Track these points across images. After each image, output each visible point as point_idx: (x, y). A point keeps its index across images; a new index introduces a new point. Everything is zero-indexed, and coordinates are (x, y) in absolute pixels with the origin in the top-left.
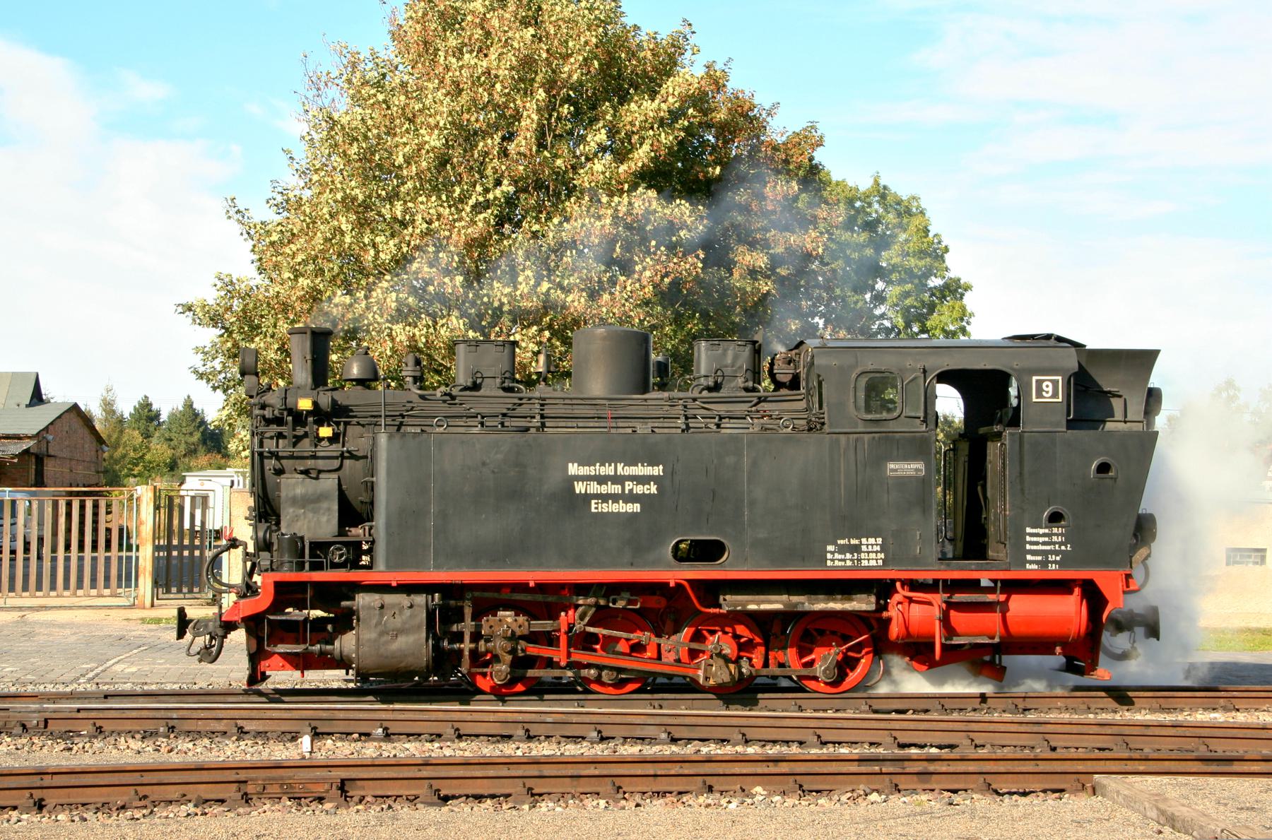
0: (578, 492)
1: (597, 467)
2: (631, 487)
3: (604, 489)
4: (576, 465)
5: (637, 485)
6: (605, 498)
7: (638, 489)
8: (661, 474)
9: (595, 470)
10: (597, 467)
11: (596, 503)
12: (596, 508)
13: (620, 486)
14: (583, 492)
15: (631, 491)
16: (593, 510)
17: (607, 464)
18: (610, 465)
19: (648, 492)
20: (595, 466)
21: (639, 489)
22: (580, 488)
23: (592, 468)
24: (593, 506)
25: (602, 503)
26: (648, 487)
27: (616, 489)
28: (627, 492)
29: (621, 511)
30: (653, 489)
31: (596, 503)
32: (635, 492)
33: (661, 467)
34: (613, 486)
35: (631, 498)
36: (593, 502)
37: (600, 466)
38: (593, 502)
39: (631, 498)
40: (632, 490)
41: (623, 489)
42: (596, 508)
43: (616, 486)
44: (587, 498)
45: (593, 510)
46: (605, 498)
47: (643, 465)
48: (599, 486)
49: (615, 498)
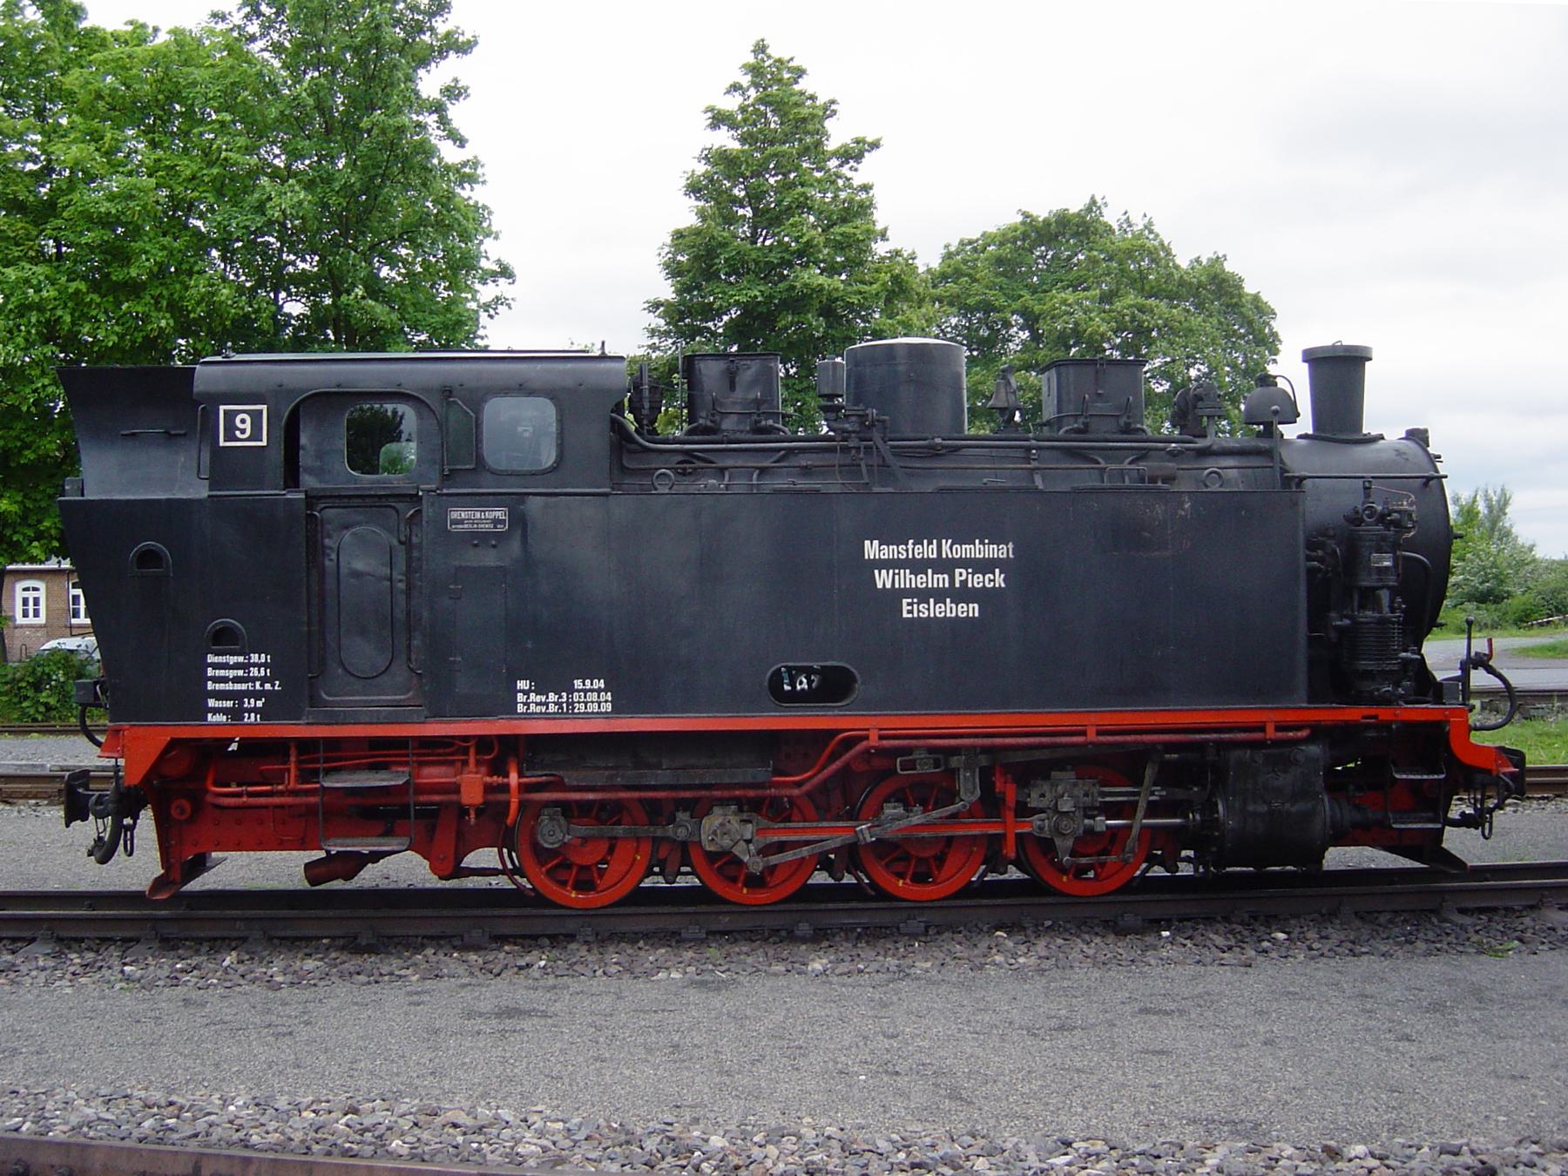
0: (880, 586)
1: (910, 546)
3: (920, 581)
4: (876, 542)
6: (923, 595)
8: (1011, 556)
9: (907, 550)
10: (910, 546)
11: (909, 604)
14: (888, 586)
16: (905, 615)
20: (907, 544)
21: (976, 581)
22: (883, 579)
24: (905, 608)
25: (918, 604)
31: (909, 604)
32: (970, 585)
33: (1011, 546)
34: (935, 576)
36: (905, 601)
37: (914, 544)
38: (905, 601)
44: (897, 595)
46: (923, 595)
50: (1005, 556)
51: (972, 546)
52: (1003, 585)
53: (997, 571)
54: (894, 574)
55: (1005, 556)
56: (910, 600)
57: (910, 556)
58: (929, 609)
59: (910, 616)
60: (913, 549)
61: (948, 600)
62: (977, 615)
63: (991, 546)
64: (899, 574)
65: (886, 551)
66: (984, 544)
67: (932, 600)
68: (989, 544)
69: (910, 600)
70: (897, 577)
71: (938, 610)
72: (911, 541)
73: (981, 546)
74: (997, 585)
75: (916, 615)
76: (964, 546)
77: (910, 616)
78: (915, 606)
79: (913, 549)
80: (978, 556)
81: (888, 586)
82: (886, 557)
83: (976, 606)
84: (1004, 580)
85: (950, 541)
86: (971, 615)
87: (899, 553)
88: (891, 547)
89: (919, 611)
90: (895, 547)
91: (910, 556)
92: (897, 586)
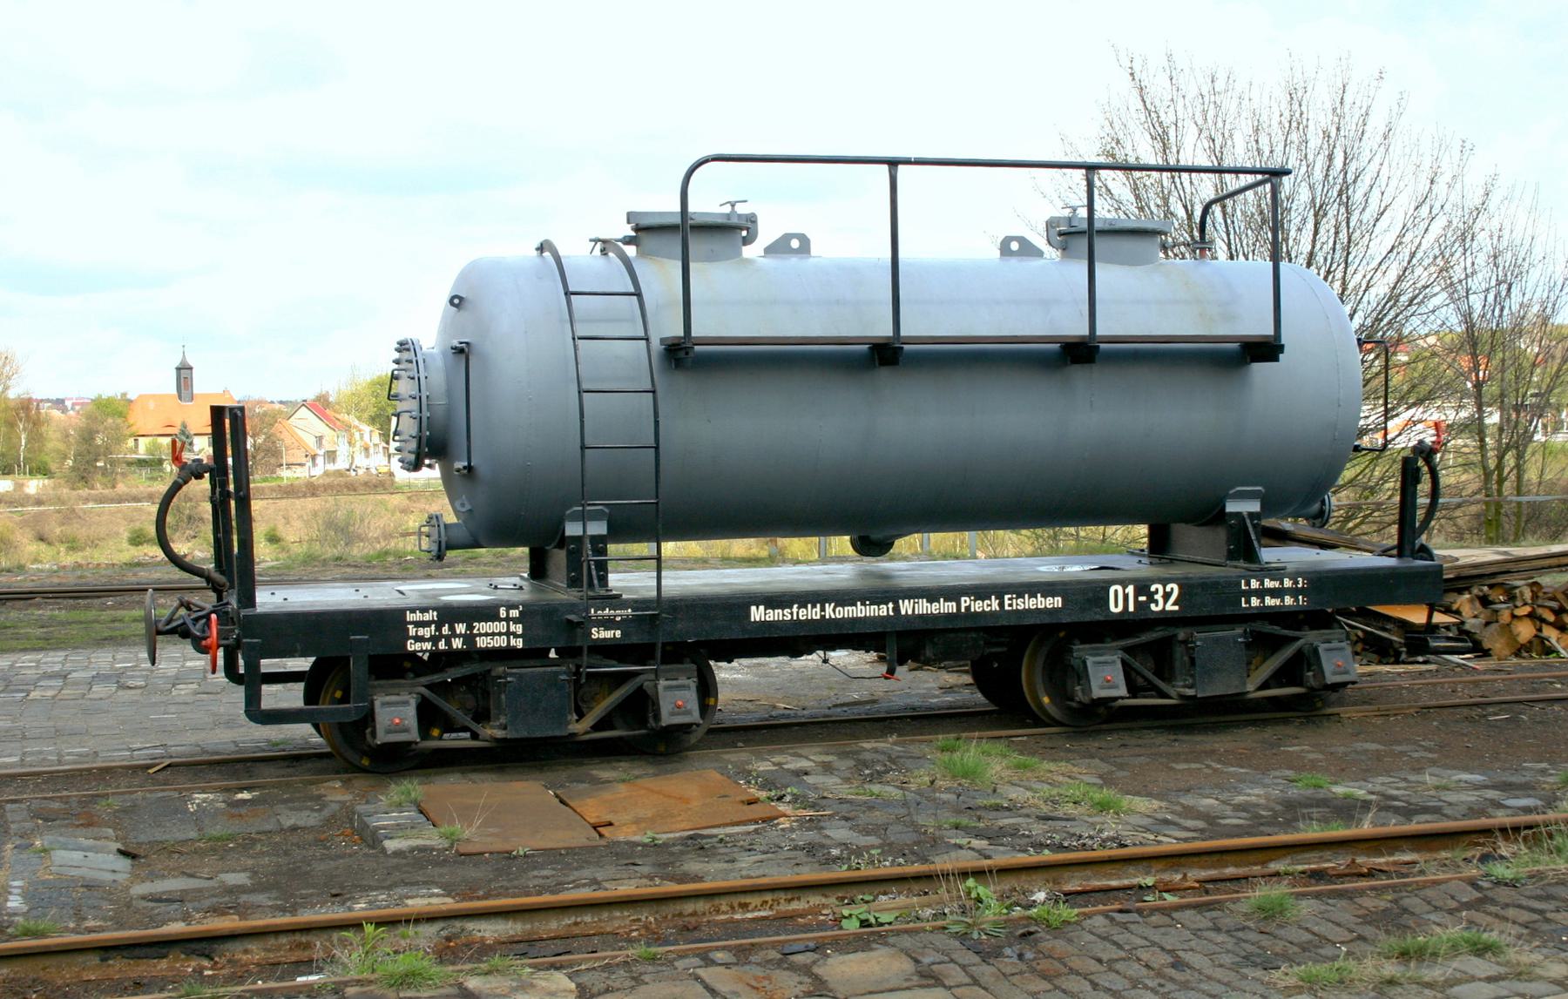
1: (795, 609)
8: (891, 613)
9: (792, 614)
17: (809, 606)
20: (791, 608)
23: (787, 611)
37: (799, 608)
47: (863, 604)
50: (885, 614)
55: (885, 614)
60: (798, 613)
63: (872, 607)
65: (771, 614)
66: (865, 605)
68: (870, 605)
73: (863, 608)
76: (846, 608)
79: (798, 613)
85: (833, 605)
87: (784, 615)
88: (776, 611)
90: (780, 611)
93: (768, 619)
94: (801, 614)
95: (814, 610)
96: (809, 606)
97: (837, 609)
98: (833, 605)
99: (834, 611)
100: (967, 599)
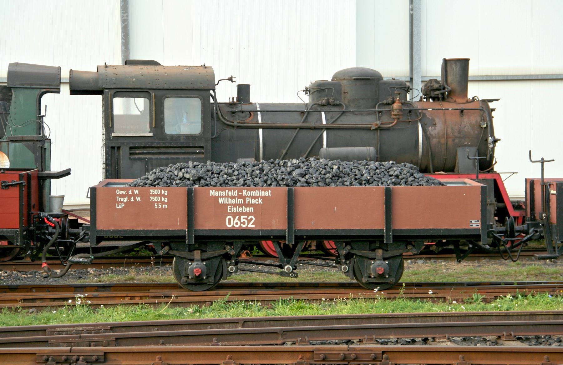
0: (220, 203)
1: (227, 192)
2: (249, 201)
3: (234, 201)
4: (214, 190)
5: (252, 199)
6: (235, 205)
7: (252, 201)
8: (270, 195)
9: (226, 193)
10: (227, 192)
11: (230, 208)
12: (230, 210)
13: (242, 200)
14: (223, 203)
15: (249, 202)
16: (229, 211)
17: (233, 190)
18: (235, 191)
19: (257, 203)
20: (225, 191)
21: (253, 201)
22: (221, 201)
23: (224, 192)
24: (229, 209)
25: (233, 207)
26: (258, 200)
27: (241, 201)
28: (247, 203)
29: (244, 211)
30: (260, 201)
31: (230, 208)
32: (250, 203)
33: (270, 192)
34: (239, 200)
35: (249, 205)
36: (229, 207)
37: (228, 191)
38: (229, 207)
39: (249, 205)
40: (249, 202)
41: (245, 201)
42: (230, 210)
43: (241, 200)
44: (225, 206)
45: (229, 211)
46: (235, 205)
47: (259, 191)
48: (231, 200)
49: (240, 206)
51: (255, 192)
52: (262, 203)
53: (260, 198)
54: (224, 199)
55: (267, 195)
56: (230, 206)
57: (227, 195)
58: (236, 209)
59: (230, 211)
60: (228, 193)
61: (243, 206)
62: (253, 211)
63: (262, 192)
64: (226, 199)
66: (259, 191)
67: (238, 206)
69: (230, 206)
70: (225, 200)
71: (240, 210)
72: (227, 190)
73: (259, 192)
74: (260, 203)
75: (232, 211)
76: (252, 192)
77: (230, 211)
78: (232, 208)
79: (228, 193)
80: (257, 195)
81: (223, 203)
82: (218, 195)
83: (252, 208)
84: (262, 201)
85: (246, 190)
86: (251, 211)
87: (222, 194)
88: (220, 192)
89: (233, 210)
90: (221, 192)
91: (227, 195)
92: (225, 203)
93: (216, 195)
94: (229, 194)
95: (235, 192)
96: (233, 190)
97: (248, 192)
98: (246, 190)
99: (246, 192)
100: (249, 198)
